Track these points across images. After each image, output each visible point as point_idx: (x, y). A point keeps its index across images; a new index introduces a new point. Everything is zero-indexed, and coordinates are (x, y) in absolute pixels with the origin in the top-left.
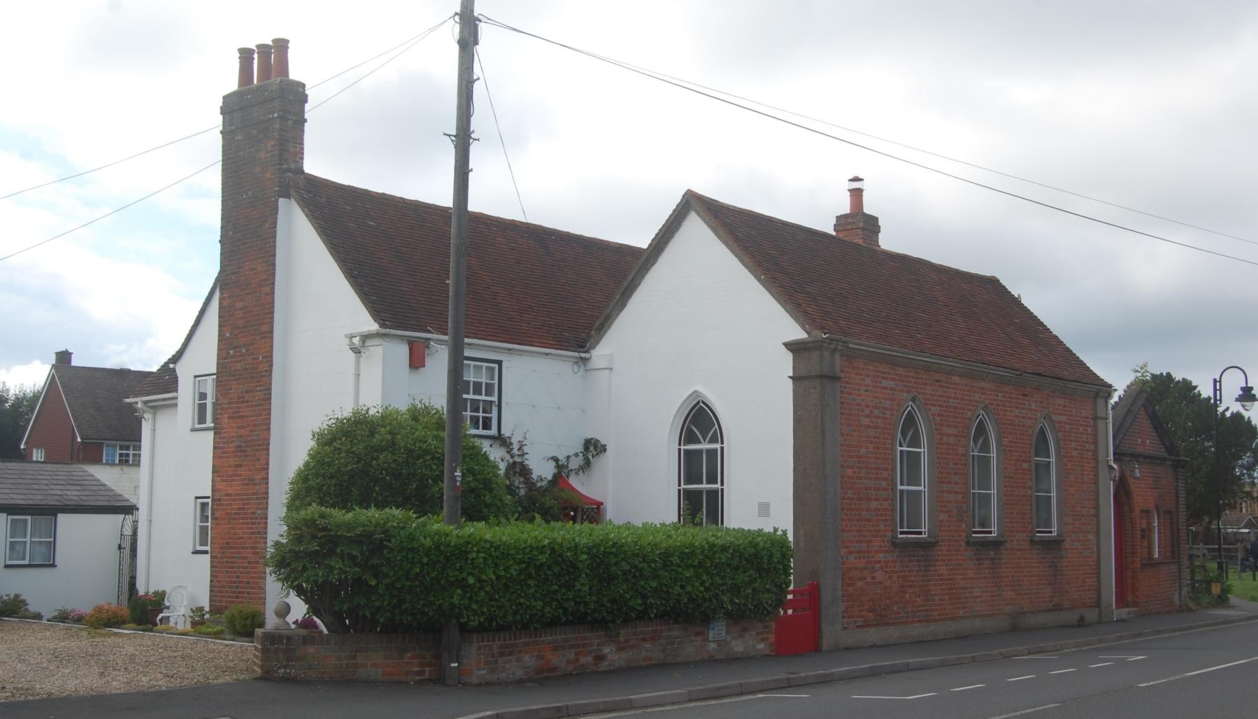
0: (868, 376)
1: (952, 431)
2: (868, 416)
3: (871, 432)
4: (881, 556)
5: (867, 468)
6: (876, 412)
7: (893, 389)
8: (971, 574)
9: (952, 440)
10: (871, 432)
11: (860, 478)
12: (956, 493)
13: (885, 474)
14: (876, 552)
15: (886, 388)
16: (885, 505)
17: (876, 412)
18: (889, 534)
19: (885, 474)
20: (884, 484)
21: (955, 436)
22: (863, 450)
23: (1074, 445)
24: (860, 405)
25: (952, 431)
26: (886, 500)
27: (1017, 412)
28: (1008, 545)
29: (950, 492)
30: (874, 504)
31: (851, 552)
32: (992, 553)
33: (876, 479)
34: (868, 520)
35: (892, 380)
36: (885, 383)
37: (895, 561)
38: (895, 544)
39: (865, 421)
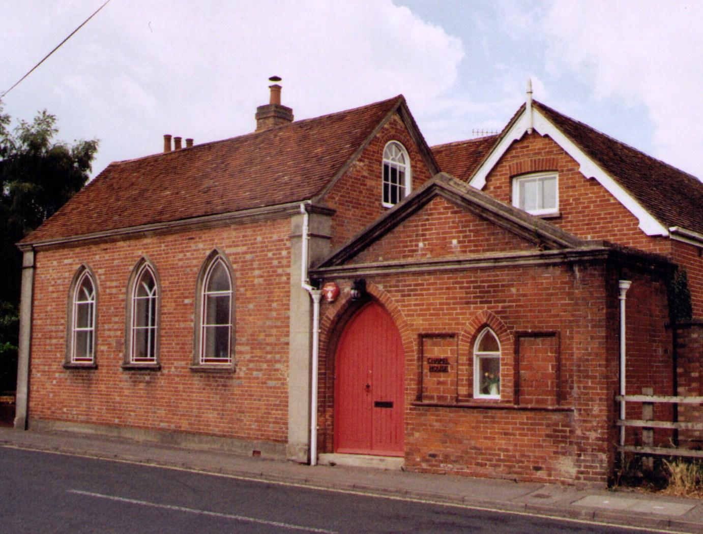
0: (55, 260)
1: (114, 284)
2: (53, 286)
3: (55, 295)
4: (57, 375)
5: (51, 318)
6: (59, 282)
7: (71, 264)
8: (127, 392)
9: (114, 291)
10: (55, 295)
11: (46, 325)
12: (116, 330)
13: (62, 321)
14: (55, 372)
15: (66, 265)
16: (61, 341)
17: (59, 282)
18: (63, 361)
19: (62, 321)
20: (61, 327)
21: (116, 287)
22: (49, 308)
23: (257, 272)
24: (48, 279)
25: (114, 284)
26: (62, 338)
27: (181, 256)
28: (165, 371)
29: (109, 330)
30: (54, 341)
31: (38, 371)
32: (147, 378)
33: (56, 325)
34: (49, 351)
35: (71, 258)
36: (66, 261)
37: (66, 379)
38: (67, 367)
39: (51, 289)
